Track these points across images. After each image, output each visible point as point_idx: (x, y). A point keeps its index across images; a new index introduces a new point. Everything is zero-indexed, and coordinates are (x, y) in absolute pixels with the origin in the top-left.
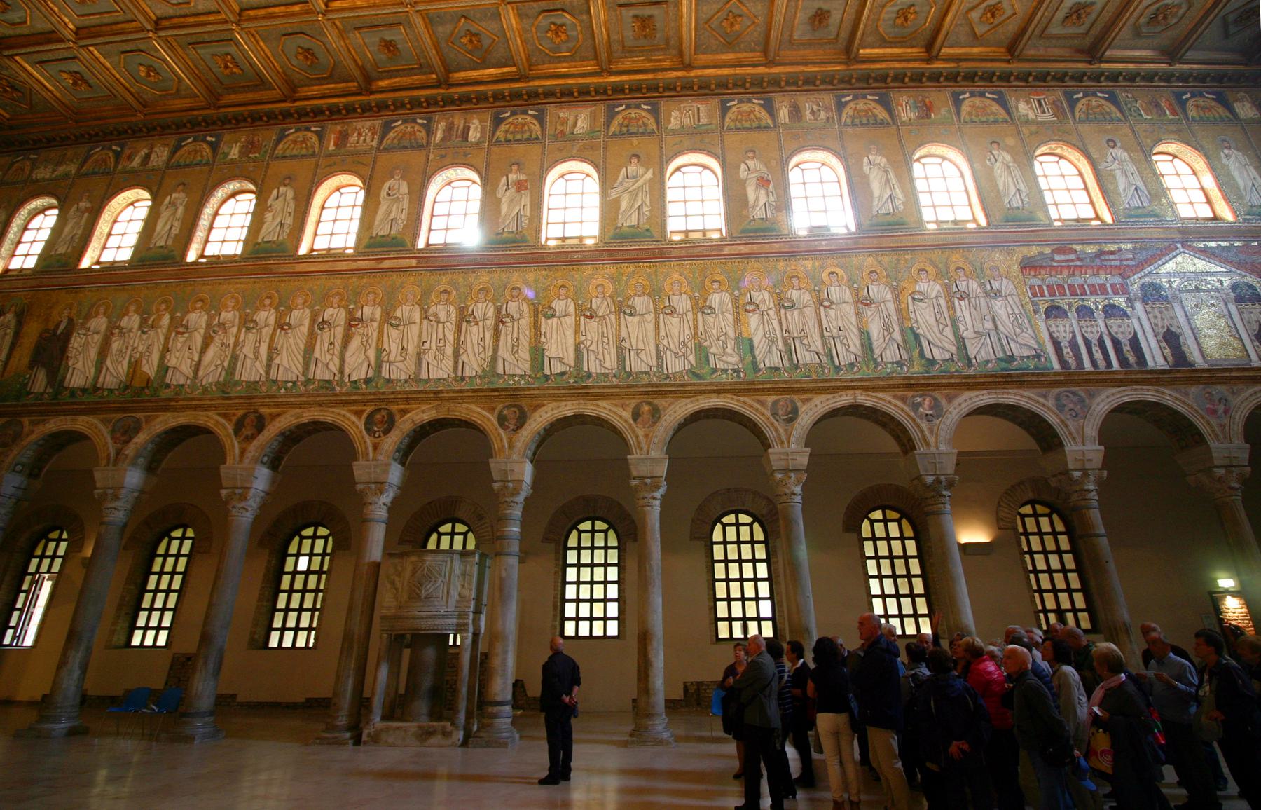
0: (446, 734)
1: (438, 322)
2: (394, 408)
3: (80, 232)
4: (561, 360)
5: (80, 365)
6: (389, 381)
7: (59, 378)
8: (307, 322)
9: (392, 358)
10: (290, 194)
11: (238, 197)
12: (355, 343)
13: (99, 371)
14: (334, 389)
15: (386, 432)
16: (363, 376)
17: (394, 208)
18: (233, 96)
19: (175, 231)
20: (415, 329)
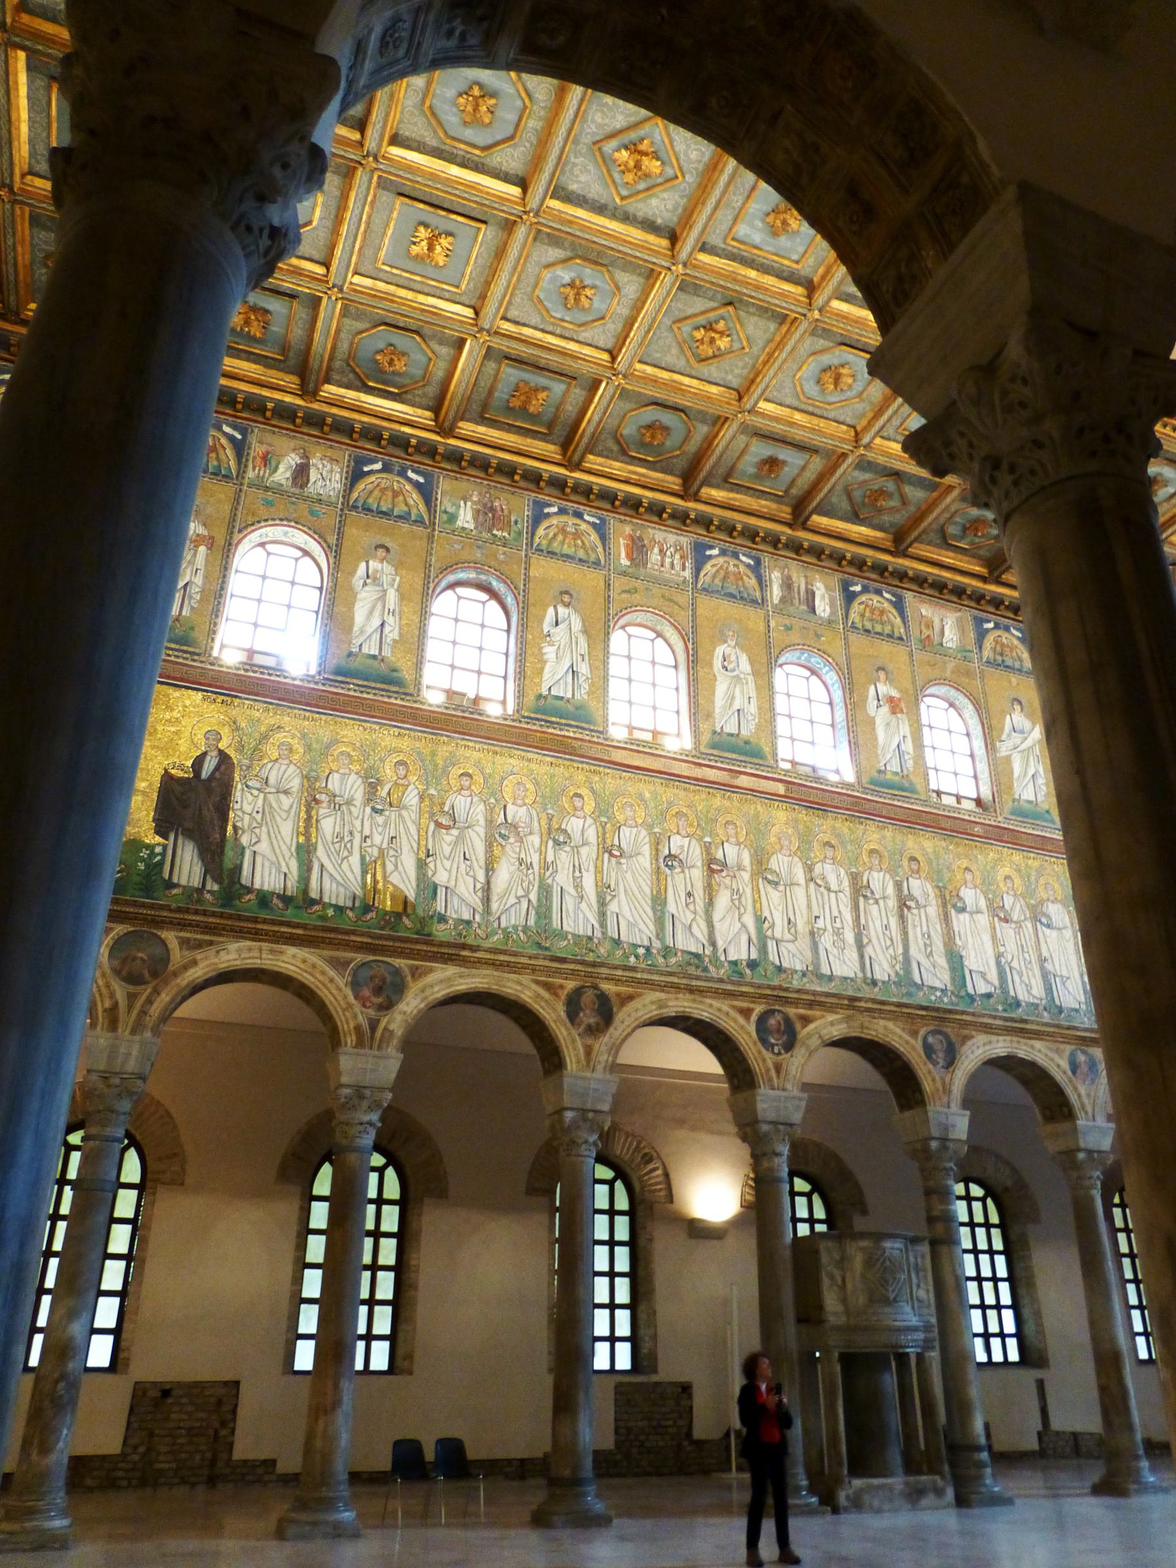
0: (939, 1493)
1: (829, 890)
2: (792, 1011)
3: (199, 580)
4: (983, 975)
5: (263, 847)
6: (780, 969)
7: (228, 864)
8: (646, 850)
9: (778, 935)
10: (577, 624)
11: (461, 591)
12: (723, 900)
13: (306, 868)
14: (706, 970)
15: (789, 1046)
16: (744, 956)
17: (737, 691)
18: (481, 429)
19: (392, 632)
20: (800, 892)
